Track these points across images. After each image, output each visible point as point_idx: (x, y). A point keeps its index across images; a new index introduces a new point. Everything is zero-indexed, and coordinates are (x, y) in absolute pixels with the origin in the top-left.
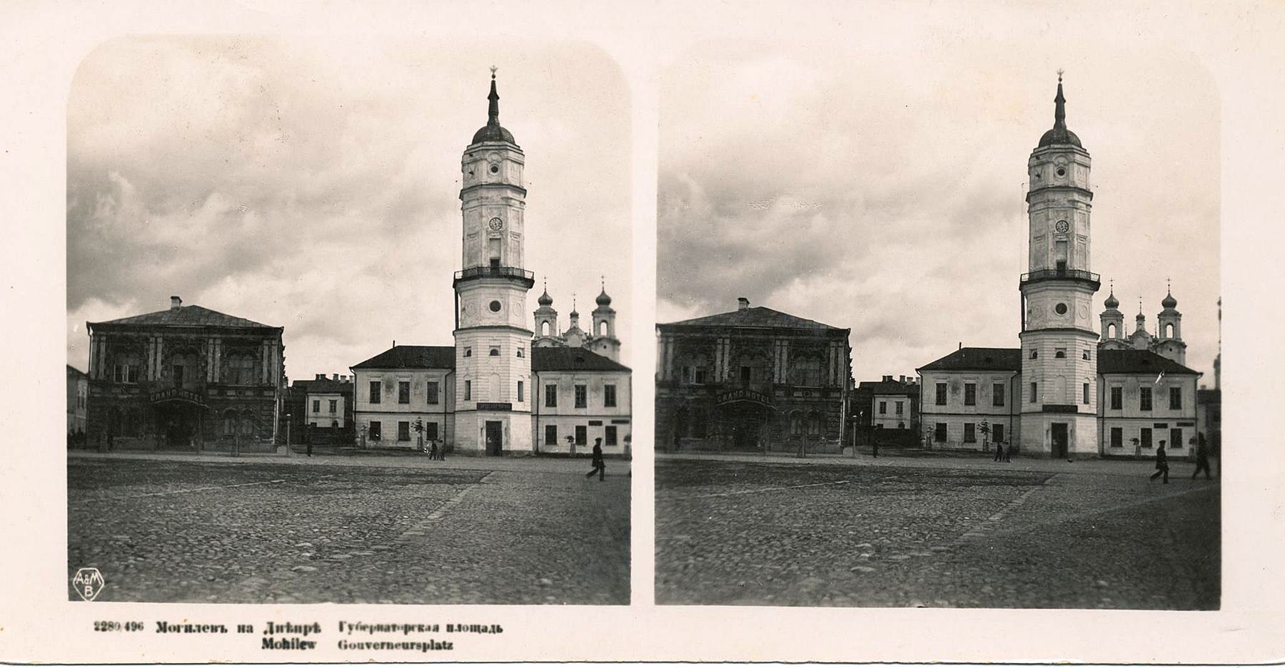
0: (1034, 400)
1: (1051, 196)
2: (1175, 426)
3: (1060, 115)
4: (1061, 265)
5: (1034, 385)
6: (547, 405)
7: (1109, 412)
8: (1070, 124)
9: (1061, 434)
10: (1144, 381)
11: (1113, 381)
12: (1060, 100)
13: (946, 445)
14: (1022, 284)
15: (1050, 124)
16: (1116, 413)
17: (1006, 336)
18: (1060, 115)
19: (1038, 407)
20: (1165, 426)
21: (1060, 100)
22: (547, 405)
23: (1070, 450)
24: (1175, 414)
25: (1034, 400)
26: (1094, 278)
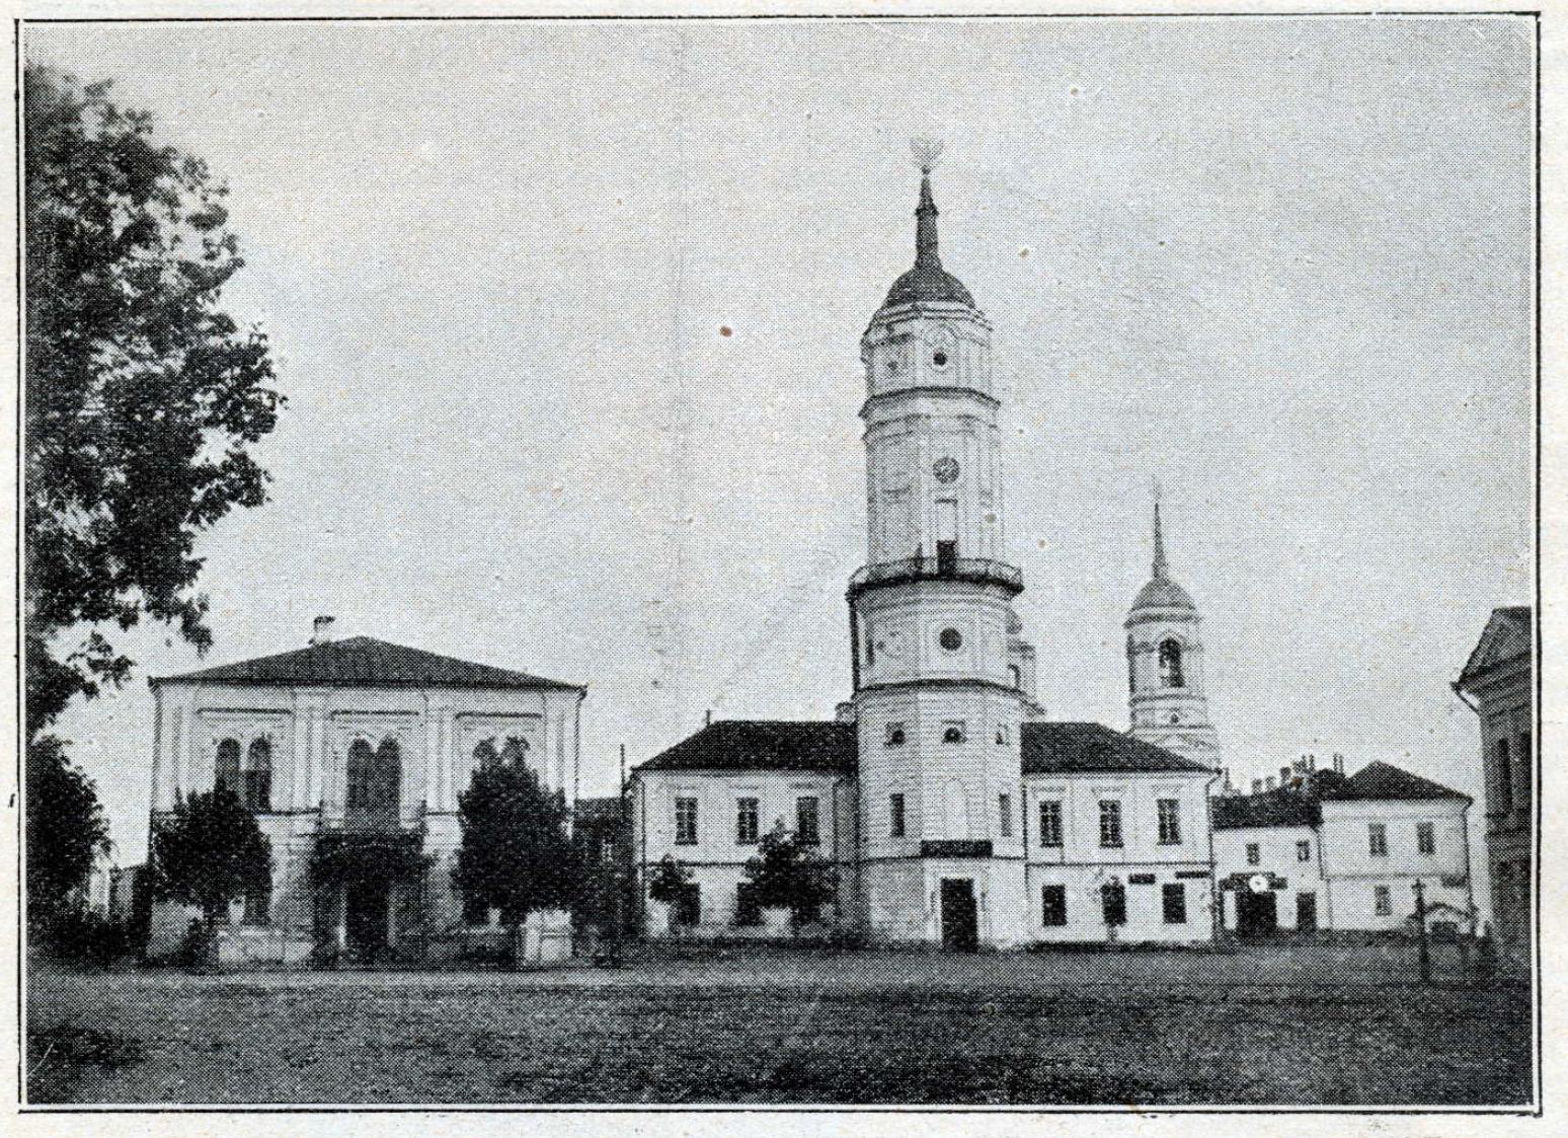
0: (899, 830)
1: (923, 405)
2: (1173, 881)
3: (926, 243)
4: (947, 550)
5: (898, 801)
6: (1045, 844)
7: (1037, 853)
8: (950, 258)
9: (958, 896)
10: (1107, 785)
11: (1048, 787)
12: (926, 211)
13: (699, 932)
14: (856, 593)
15: (908, 263)
16: (1052, 855)
17: (812, 696)
18: (926, 243)
19: (913, 849)
20: (1149, 880)
21: (926, 211)
22: (1045, 844)
23: (982, 934)
24: (1172, 853)
25: (899, 830)
26: (1008, 574)
